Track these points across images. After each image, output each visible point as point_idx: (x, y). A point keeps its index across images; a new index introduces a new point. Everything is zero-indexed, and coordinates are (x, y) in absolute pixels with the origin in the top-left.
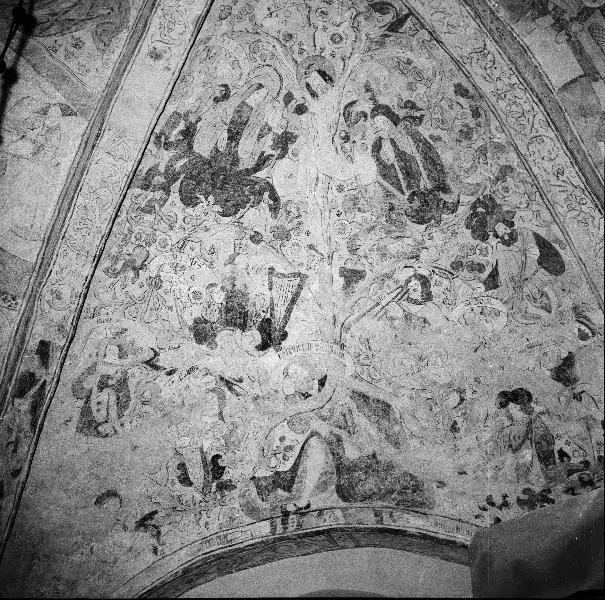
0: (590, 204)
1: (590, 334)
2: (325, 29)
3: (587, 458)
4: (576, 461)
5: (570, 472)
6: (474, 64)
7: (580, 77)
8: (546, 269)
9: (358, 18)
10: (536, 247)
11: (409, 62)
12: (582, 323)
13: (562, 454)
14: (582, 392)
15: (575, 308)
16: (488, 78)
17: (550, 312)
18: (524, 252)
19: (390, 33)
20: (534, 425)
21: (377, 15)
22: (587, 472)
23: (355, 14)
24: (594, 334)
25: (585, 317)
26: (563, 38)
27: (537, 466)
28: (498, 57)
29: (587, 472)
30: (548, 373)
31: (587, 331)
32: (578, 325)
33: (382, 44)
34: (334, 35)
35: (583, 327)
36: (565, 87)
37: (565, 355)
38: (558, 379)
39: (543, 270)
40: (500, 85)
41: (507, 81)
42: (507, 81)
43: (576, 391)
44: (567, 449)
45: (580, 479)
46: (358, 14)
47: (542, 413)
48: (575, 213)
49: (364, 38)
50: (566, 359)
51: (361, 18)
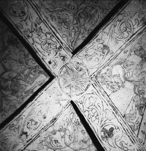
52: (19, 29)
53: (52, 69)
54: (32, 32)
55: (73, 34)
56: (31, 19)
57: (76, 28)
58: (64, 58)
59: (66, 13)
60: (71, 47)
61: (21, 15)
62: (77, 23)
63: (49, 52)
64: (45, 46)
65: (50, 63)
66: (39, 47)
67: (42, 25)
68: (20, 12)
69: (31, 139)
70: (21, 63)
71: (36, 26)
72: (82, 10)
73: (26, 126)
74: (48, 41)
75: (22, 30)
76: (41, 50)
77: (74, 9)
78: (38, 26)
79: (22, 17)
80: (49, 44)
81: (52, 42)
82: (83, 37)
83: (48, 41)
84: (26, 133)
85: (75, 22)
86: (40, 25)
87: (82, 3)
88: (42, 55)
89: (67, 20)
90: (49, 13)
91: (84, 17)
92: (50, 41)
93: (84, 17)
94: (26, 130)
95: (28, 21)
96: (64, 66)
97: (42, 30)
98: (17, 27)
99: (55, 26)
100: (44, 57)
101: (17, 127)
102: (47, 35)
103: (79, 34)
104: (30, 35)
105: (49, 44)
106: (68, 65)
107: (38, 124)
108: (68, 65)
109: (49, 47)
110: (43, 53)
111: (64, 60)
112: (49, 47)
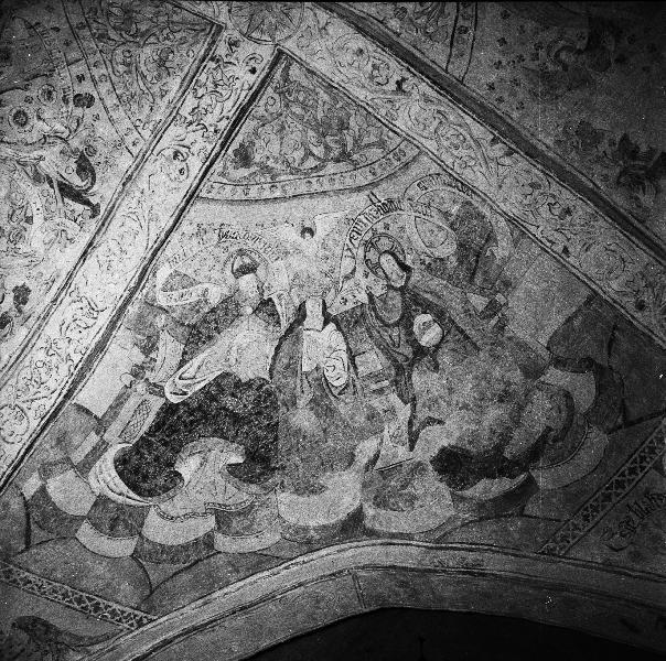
2: (28, 100)
6: (74, 306)
7: (95, 417)
9: (59, 141)
11: (29, 220)
16: (64, 327)
19: (55, 185)
21: (74, 166)
23: (64, 136)
26: (127, 379)
28: (96, 328)
33: (37, 178)
34: (25, 114)
36: (80, 409)
40: (62, 344)
41: (71, 351)
42: (71, 351)
46: (65, 141)
49: (35, 154)
51: (59, 146)
52: (210, 154)
53: (265, 61)
54: (205, 127)
55: (178, 36)
56: (183, 137)
57: (165, 32)
58: (233, 44)
59: (142, 65)
60: (208, 30)
61: (181, 158)
62: (154, 34)
63: (231, 80)
64: (224, 93)
65: (253, 71)
66: (229, 104)
67: (185, 111)
68: (176, 162)
69: (408, 70)
70: (283, 128)
71: (190, 123)
72: (123, 33)
73: (384, 87)
74: (209, 89)
75: (210, 147)
76: (233, 98)
77: (129, 52)
78: (190, 118)
79: (185, 155)
80: (216, 86)
81: (211, 79)
82: (175, 12)
83: (209, 89)
84: (397, 82)
85: (152, 39)
86: (187, 115)
87: (109, 39)
88: (244, 93)
89: (156, 58)
90: (158, 100)
91: (134, 26)
92: (210, 86)
93: (134, 26)
94: (392, 86)
95: (186, 142)
96: (250, 38)
97: (193, 110)
98: (207, 158)
99: (179, 80)
100: (246, 87)
101: (389, 106)
102: (199, 95)
103: (172, 22)
104: (212, 129)
105: (216, 86)
106: (245, 30)
107: (378, 62)
108: (245, 30)
109: (221, 83)
110: (239, 91)
111: (236, 42)
112: (221, 83)
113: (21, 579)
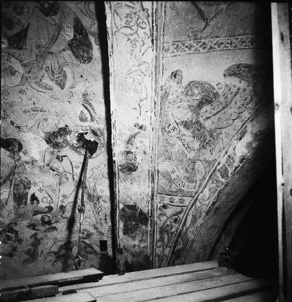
0: (147, 31)
1: (89, 119)
3: (52, 205)
4: (43, 205)
5: (36, 213)
8: (73, 52)
10: (72, 29)
12: (86, 108)
13: (34, 198)
14: (65, 156)
15: (85, 95)
17: (62, 89)
18: (60, 29)
20: (17, 170)
22: (49, 215)
24: (92, 120)
25: (90, 105)
27: (11, 203)
29: (49, 215)
30: (43, 135)
31: (88, 116)
32: (82, 108)
35: (85, 111)
37: (63, 126)
38: (48, 141)
39: (70, 52)
43: (60, 154)
44: (38, 195)
45: (42, 219)
47: (27, 163)
48: (128, 31)
50: (61, 129)
113: (215, 44)
